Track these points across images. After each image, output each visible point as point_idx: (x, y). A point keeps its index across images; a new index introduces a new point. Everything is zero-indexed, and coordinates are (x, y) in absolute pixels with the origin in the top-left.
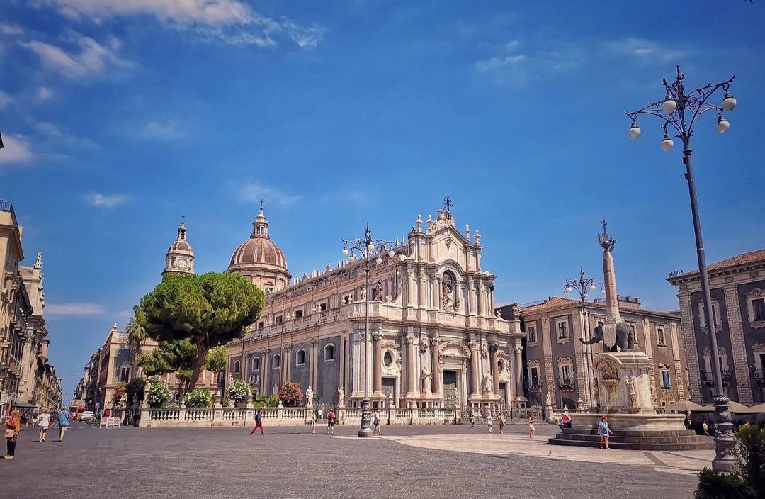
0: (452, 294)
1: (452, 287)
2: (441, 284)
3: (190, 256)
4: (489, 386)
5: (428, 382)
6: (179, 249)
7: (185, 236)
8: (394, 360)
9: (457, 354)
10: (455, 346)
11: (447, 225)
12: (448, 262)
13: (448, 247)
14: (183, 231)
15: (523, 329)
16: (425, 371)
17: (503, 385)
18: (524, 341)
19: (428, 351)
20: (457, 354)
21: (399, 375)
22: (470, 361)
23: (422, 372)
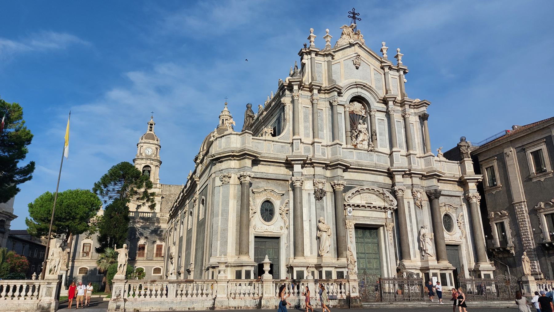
0: (366, 126)
1: (368, 118)
2: (347, 114)
3: (156, 144)
4: (430, 247)
5: (329, 242)
6: (146, 139)
7: (153, 128)
8: (277, 211)
9: (379, 202)
10: (370, 191)
11: (352, 41)
12: (357, 85)
13: (357, 68)
14: (151, 124)
15: (477, 171)
16: (320, 225)
17: (455, 247)
18: (480, 187)
19: (328, 200)
20: (379, 202)
21: (284, 232)
22: (397, 212)
23: (318, 229)
